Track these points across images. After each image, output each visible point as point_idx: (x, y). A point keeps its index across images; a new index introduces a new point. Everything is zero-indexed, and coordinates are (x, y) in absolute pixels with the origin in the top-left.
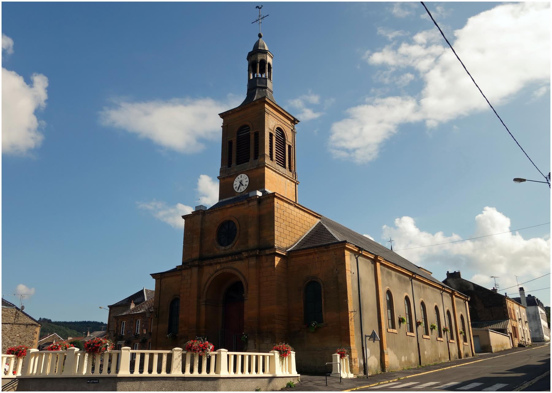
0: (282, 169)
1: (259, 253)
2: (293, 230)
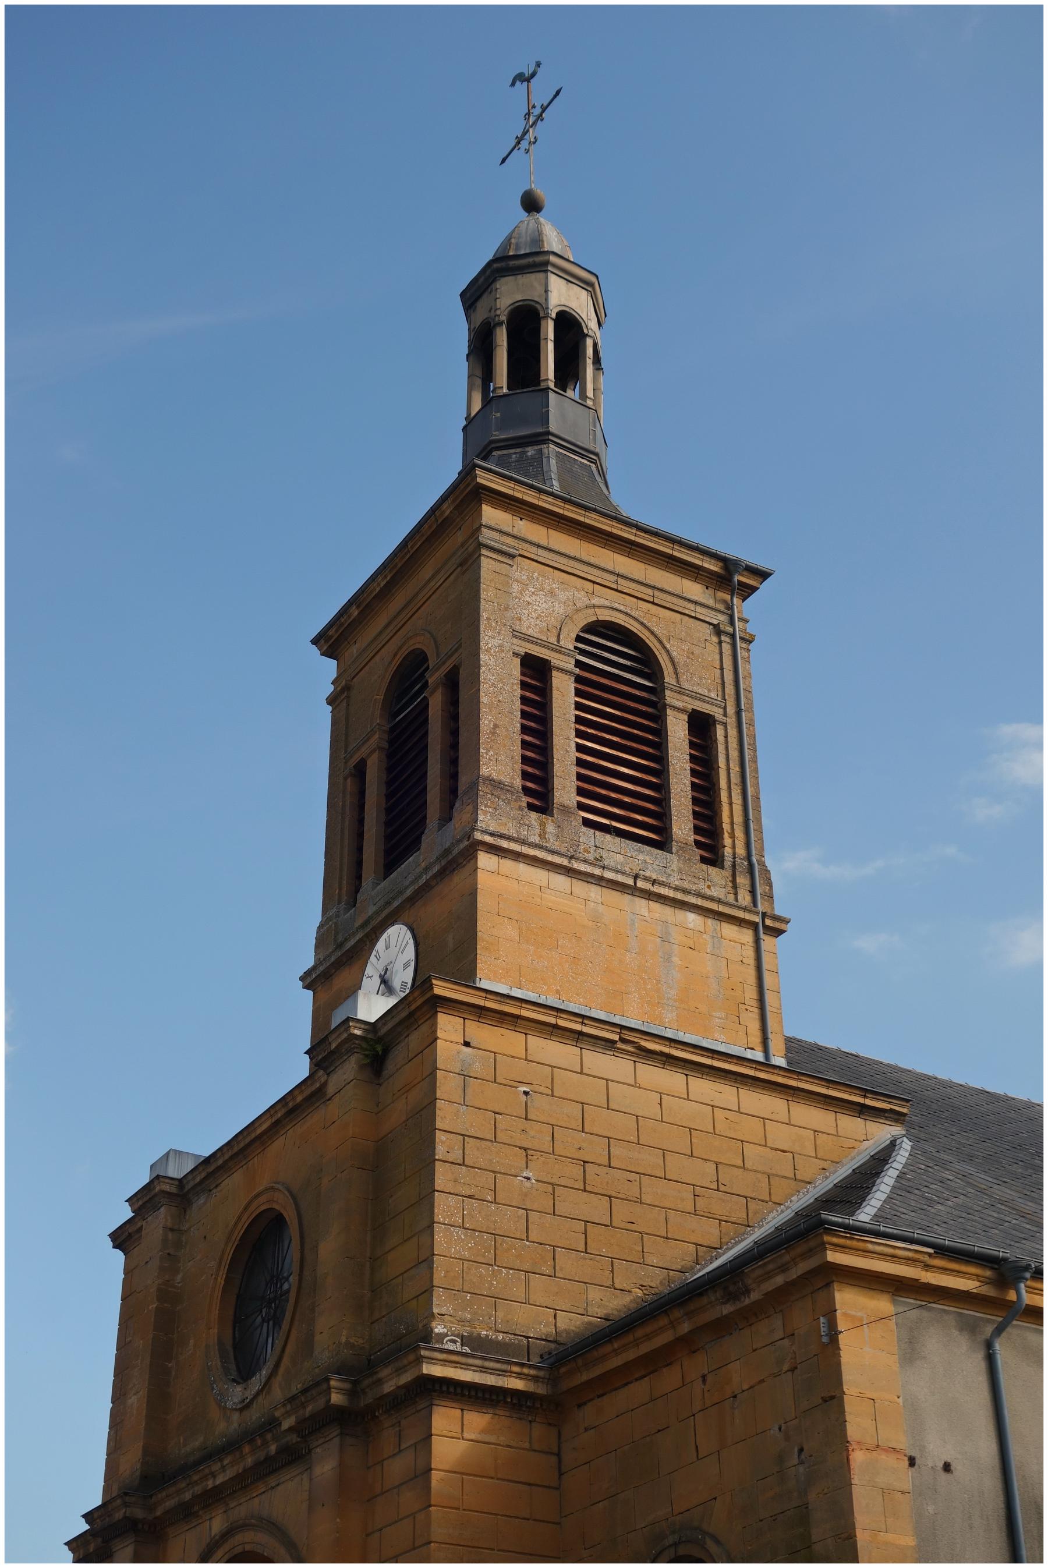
0: (646, 860)
1: (352, 1393)
2: (623, 1212)
